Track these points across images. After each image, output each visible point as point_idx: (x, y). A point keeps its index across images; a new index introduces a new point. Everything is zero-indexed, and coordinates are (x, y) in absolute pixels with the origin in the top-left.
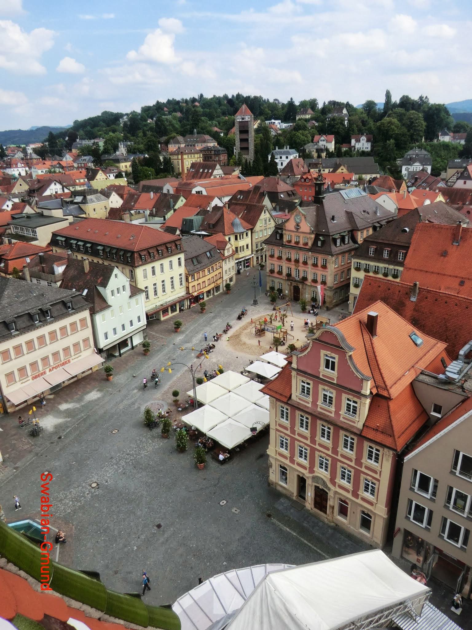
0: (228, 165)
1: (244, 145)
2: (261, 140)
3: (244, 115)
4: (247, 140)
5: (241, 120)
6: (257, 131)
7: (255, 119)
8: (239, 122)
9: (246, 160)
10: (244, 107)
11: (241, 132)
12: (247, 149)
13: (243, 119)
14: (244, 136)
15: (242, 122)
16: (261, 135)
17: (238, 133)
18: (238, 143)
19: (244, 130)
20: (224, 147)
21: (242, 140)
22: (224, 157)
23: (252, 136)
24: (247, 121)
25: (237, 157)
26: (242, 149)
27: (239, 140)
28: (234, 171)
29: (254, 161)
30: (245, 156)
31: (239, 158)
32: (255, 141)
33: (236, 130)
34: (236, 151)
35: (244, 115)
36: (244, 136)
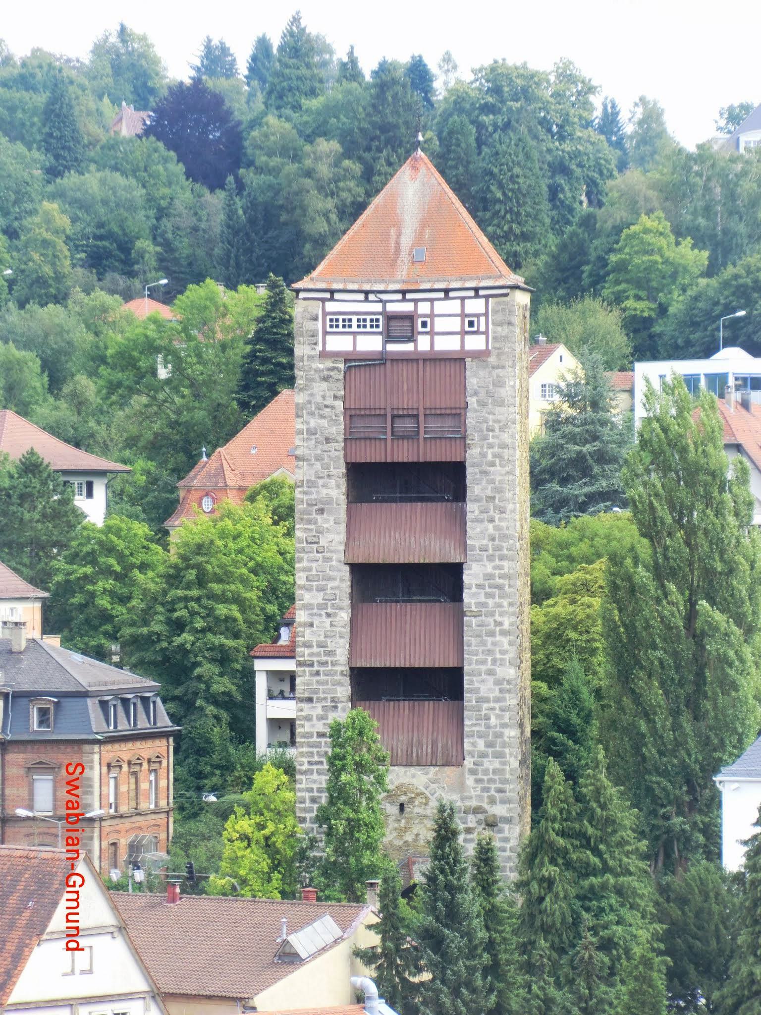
0: (194, 883)
1: (408, 636)
2: (622, 590)
3: (408, 273)
4: (442, 582)
5: (371, 344)
6: (566, 473)
7: (542, 335)
8: (355, 363)
9: (445, 834)
10: (415, 189)
11: (373, 481)
12: (443, 685)
13: (399, 326)
14: (408, 535)
15: (381, 360)
16: (615, 524)
17: (336, 490)
18: (324, 626)
19: (406, 473)
20: (142, 653)
21: (375, 581)
22: (130, 785)
23: (498, 538)
24: (456, 361)
25: (314, 782)
26: (372, 684)
27: (341, 582)
28: (288, 958)
29: (536, 851)
30: (415, 778)
31: (338, 794)
32: (540, 595)
33: (298, 444)
34: (305, 692)
35: (408, 273)
36: (408, 535)
